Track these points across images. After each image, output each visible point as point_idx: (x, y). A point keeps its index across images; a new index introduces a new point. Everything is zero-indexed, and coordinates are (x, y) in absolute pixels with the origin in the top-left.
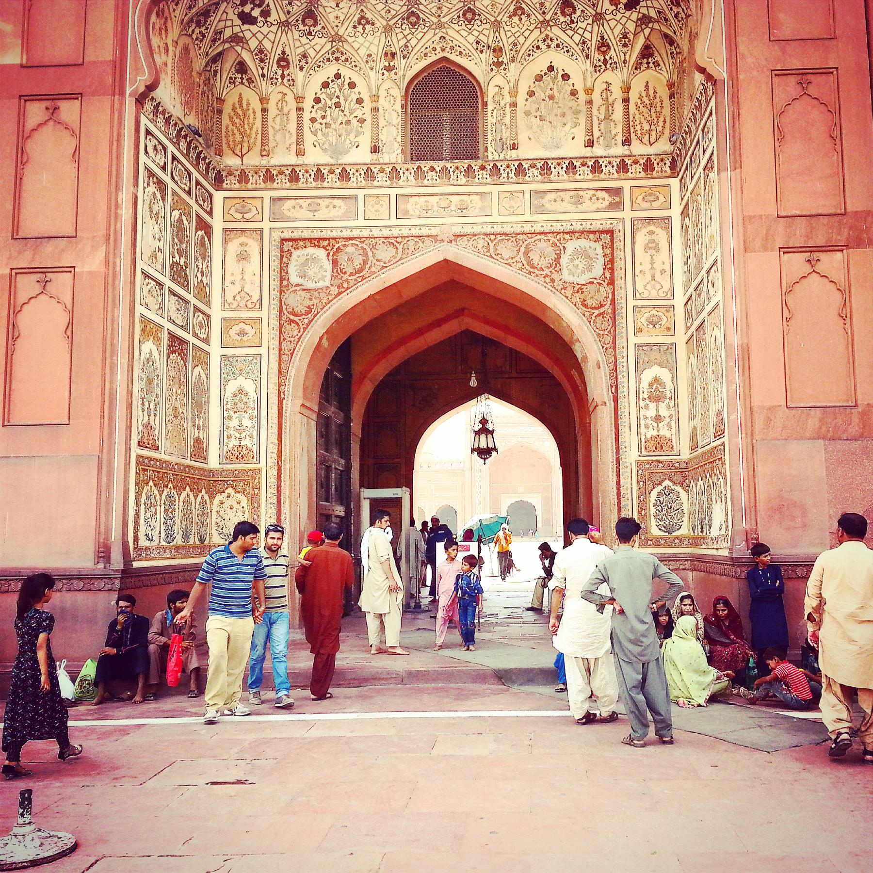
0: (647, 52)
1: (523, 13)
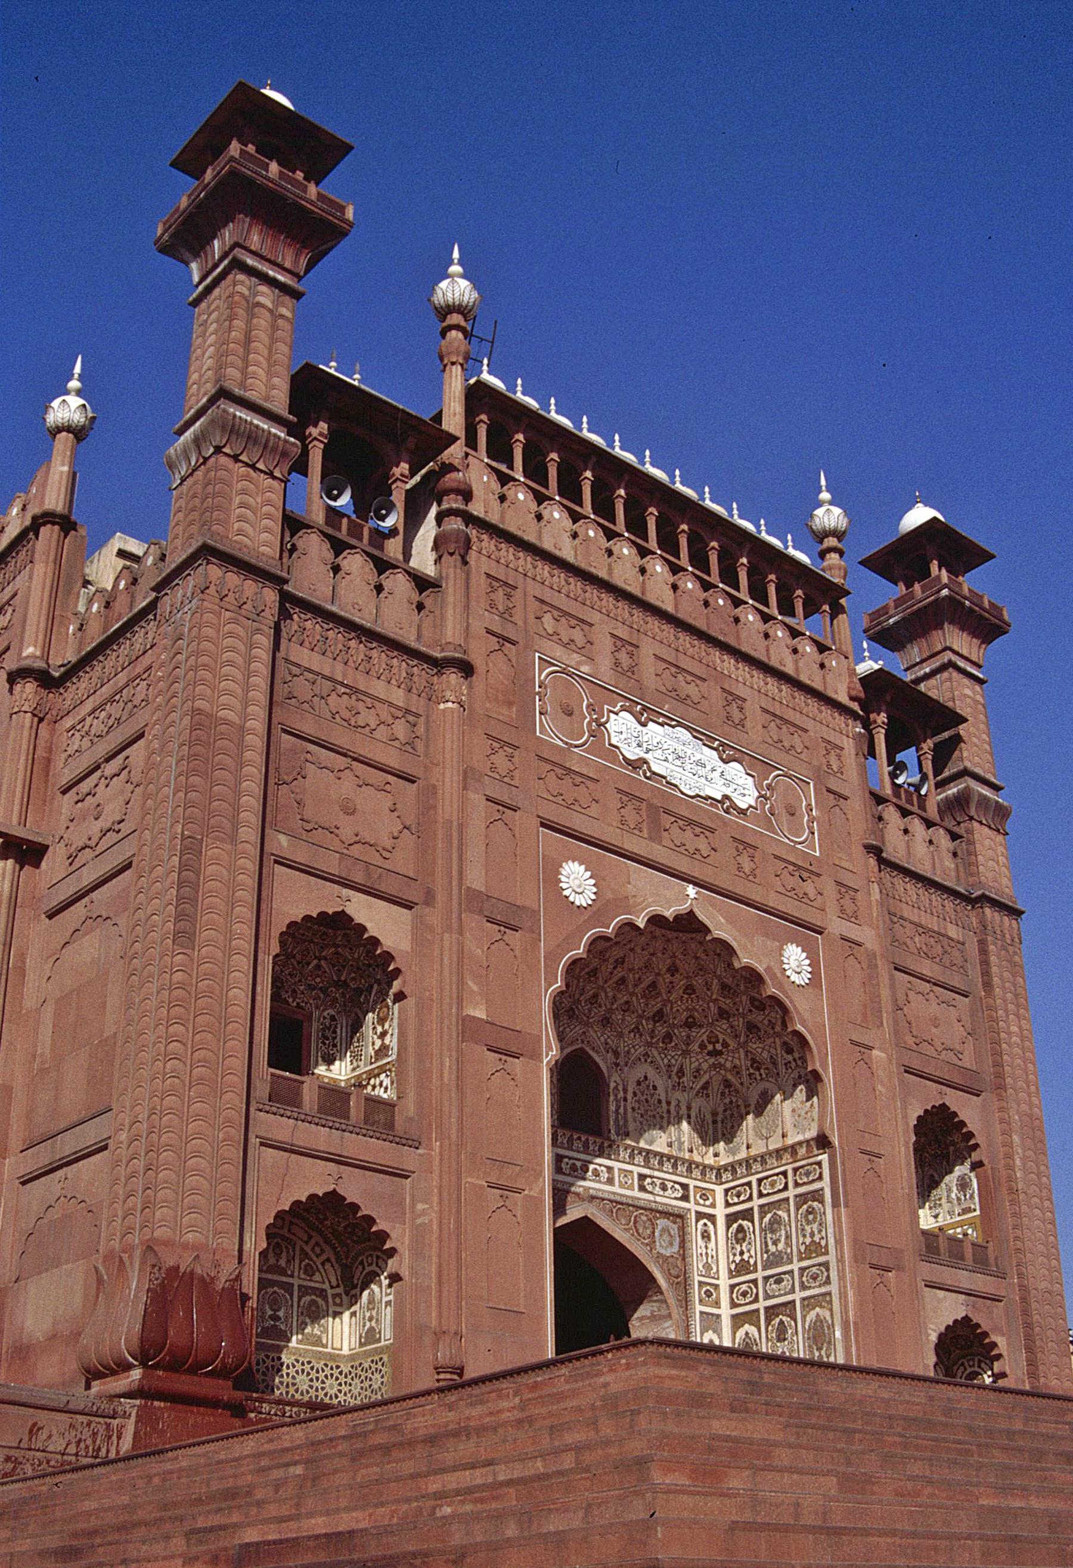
0: (706, 1086)
1: (639, 1031)
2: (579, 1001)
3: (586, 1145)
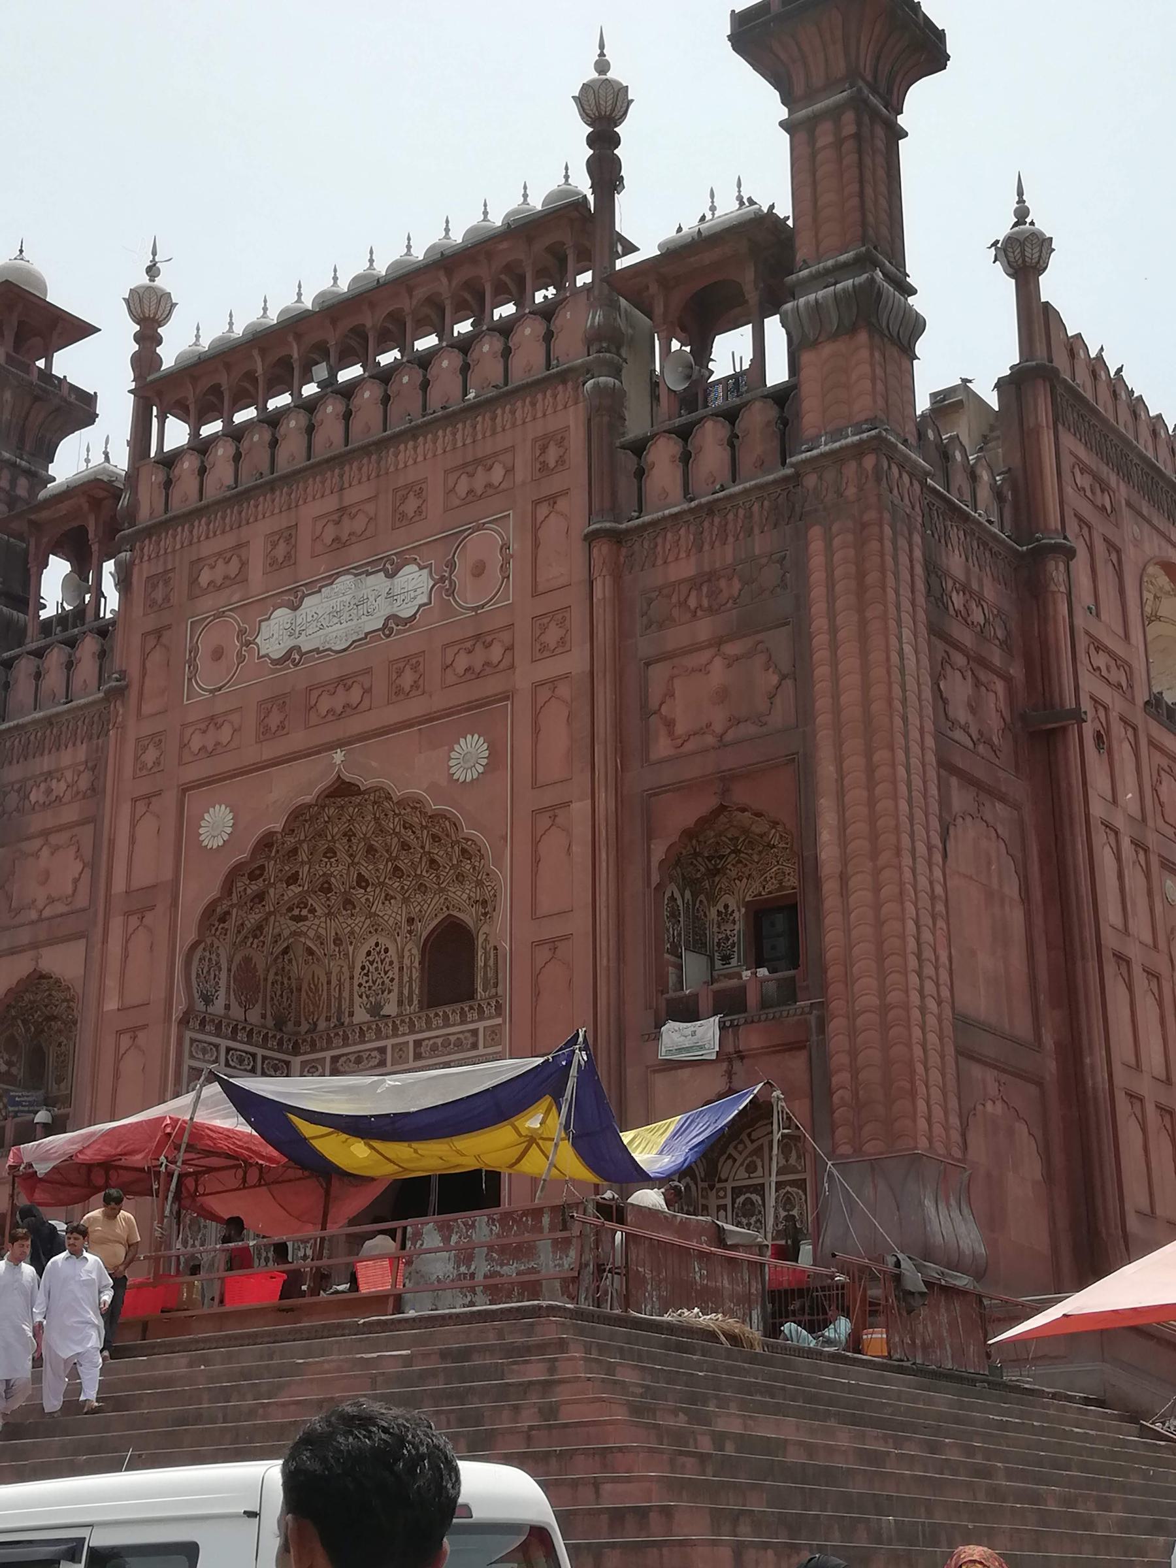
3: (446, 1017)
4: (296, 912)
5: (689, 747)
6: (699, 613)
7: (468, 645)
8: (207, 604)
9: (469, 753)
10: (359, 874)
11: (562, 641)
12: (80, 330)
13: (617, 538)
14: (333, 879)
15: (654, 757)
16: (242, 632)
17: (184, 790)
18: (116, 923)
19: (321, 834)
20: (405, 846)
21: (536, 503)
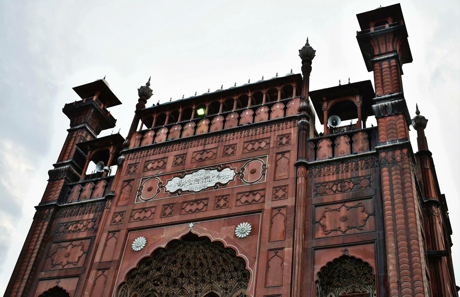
1: (233, 277)
2: (204, 277)
4: (156, 282)
5: (330, 235)
6: (337, 192)
7: (247, 194)
8: (150, 173)
9: (244, 228)
10: (182, 272)
11: (284, 196)
12: (116, 102)
13: (307, 166)
14: (172, 273)
15: (317, 237)
16: (160, 183)
17: (130, 230)
18: (93, 273)
19: (174, 254)
20: (201, 265)
21: (277, 154)
